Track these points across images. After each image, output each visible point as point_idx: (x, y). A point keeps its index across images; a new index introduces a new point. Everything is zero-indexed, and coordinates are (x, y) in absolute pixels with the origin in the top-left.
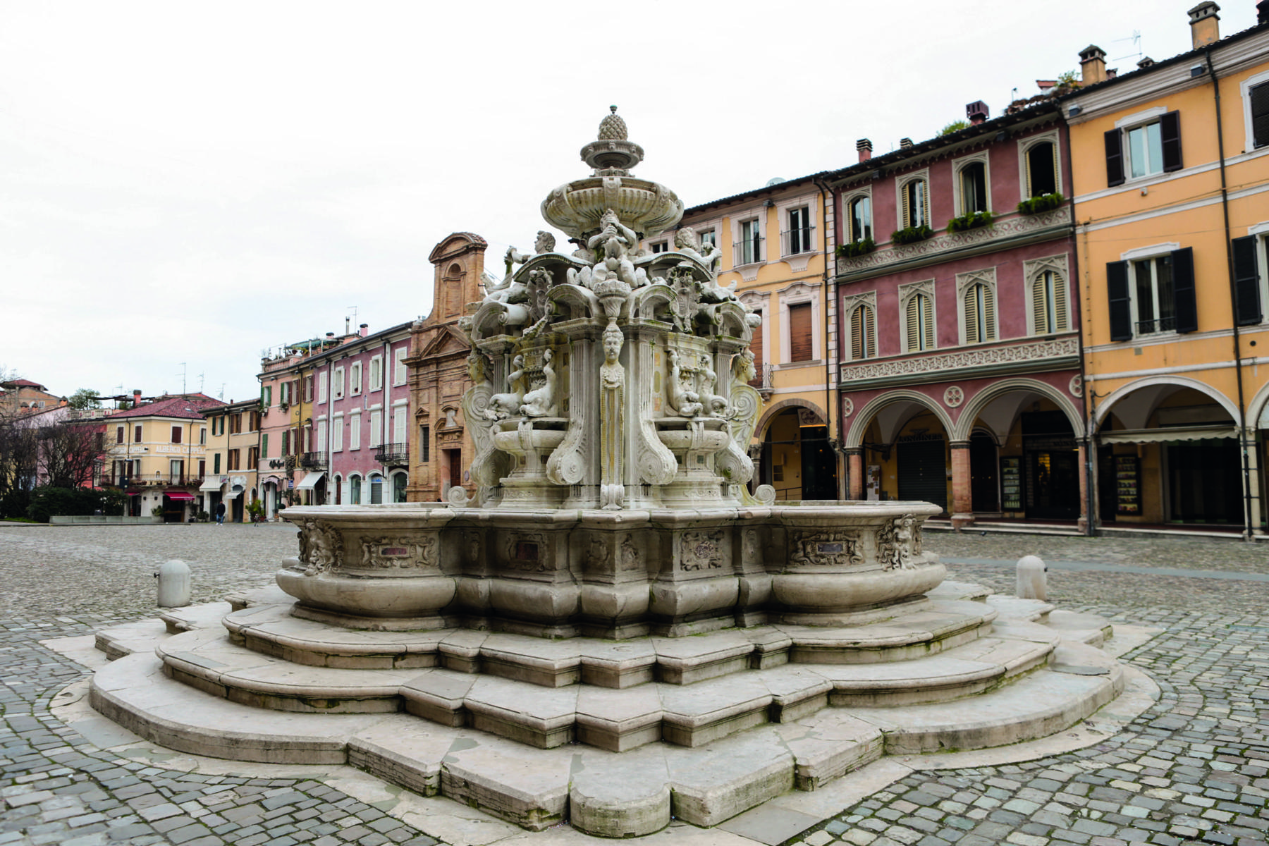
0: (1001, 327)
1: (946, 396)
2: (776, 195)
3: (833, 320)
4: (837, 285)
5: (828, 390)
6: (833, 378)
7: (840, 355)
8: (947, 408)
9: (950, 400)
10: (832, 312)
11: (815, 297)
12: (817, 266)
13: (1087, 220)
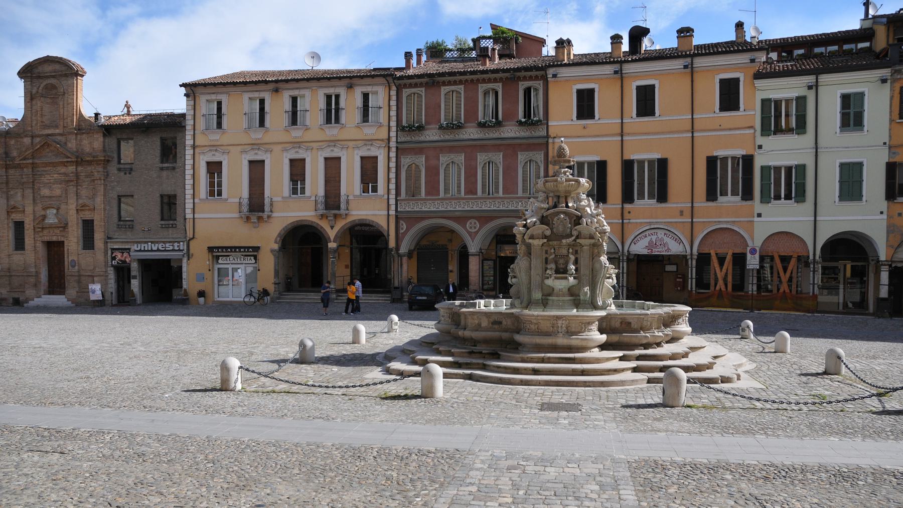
0: (503, 188)
1: (468, 223)
2: (355, 81)
3: (393, 170)
5: (388, 215)
6: (393, 207)
7: (398, 193)
9: (471, 228)
10: (393, 165)
11: (380, 154)
13: (555, 135)
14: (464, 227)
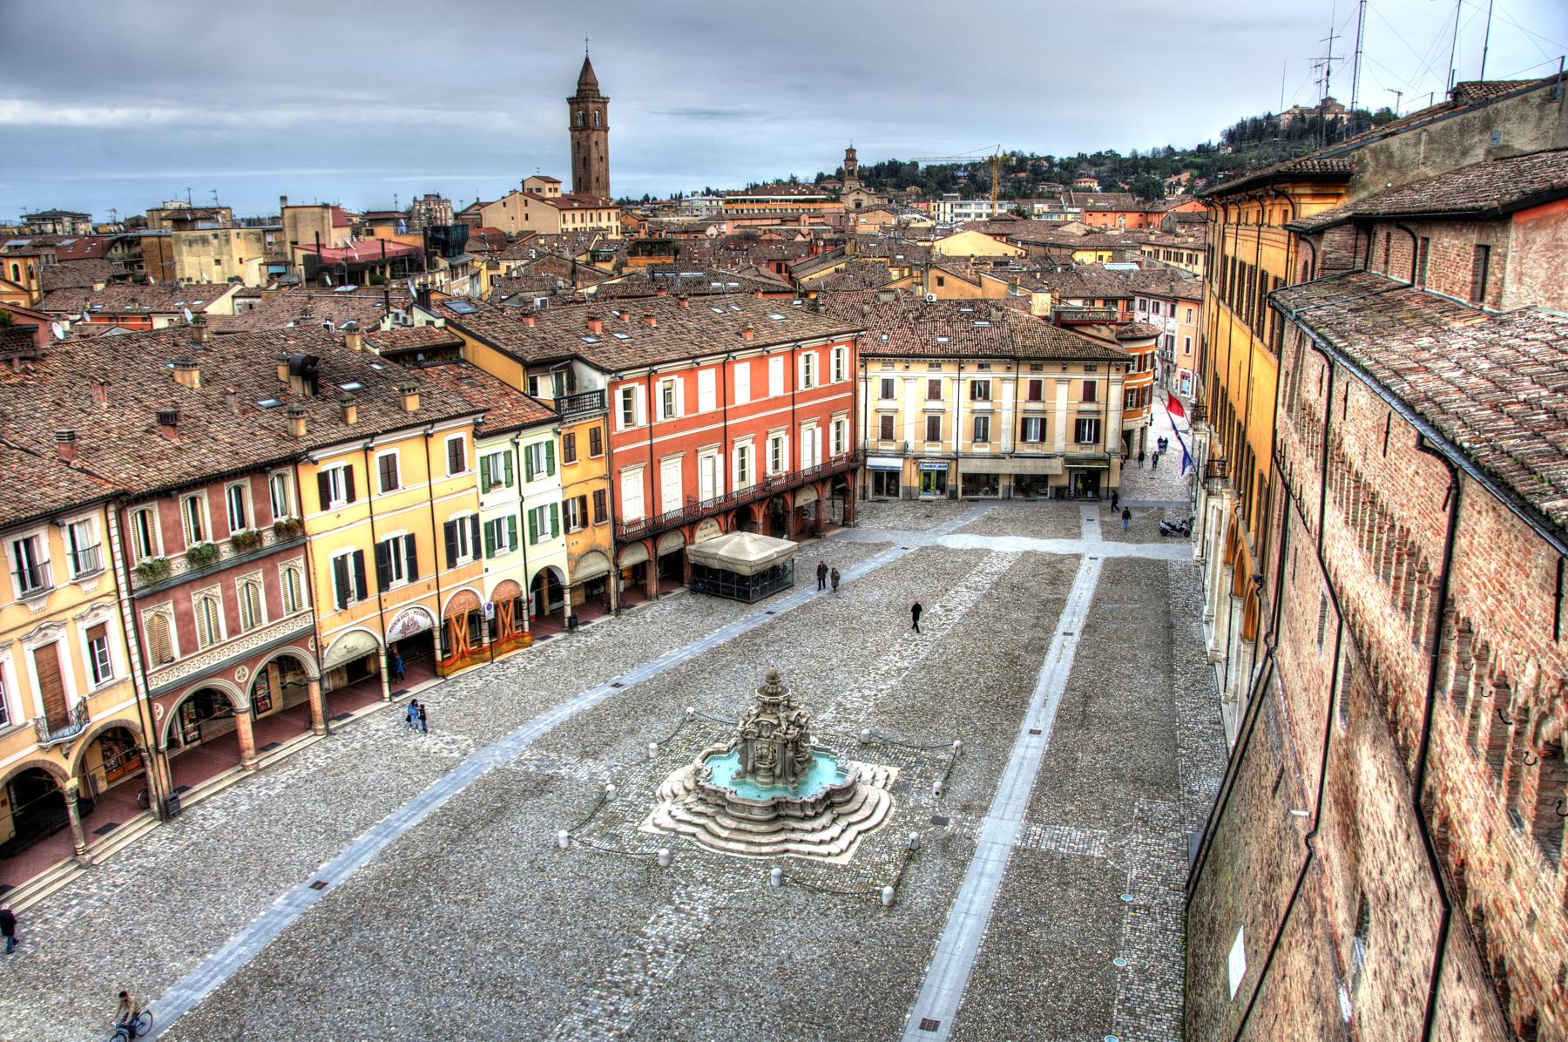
3: (131, 634)
4: (133, 601)
5: (139, 702)
6: (142, 689)
7: (144, 668)
8: (239, 685)
10: (130, 626)
12: (108, 584)
14: (234, 681)
